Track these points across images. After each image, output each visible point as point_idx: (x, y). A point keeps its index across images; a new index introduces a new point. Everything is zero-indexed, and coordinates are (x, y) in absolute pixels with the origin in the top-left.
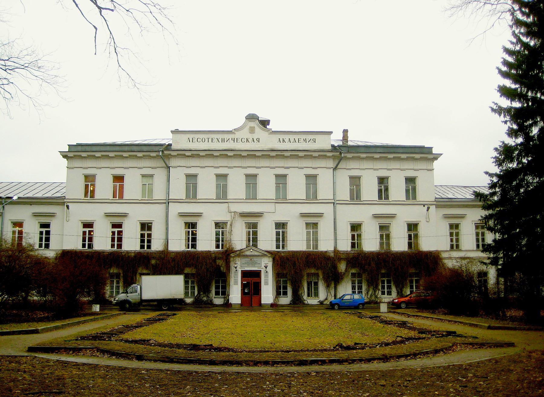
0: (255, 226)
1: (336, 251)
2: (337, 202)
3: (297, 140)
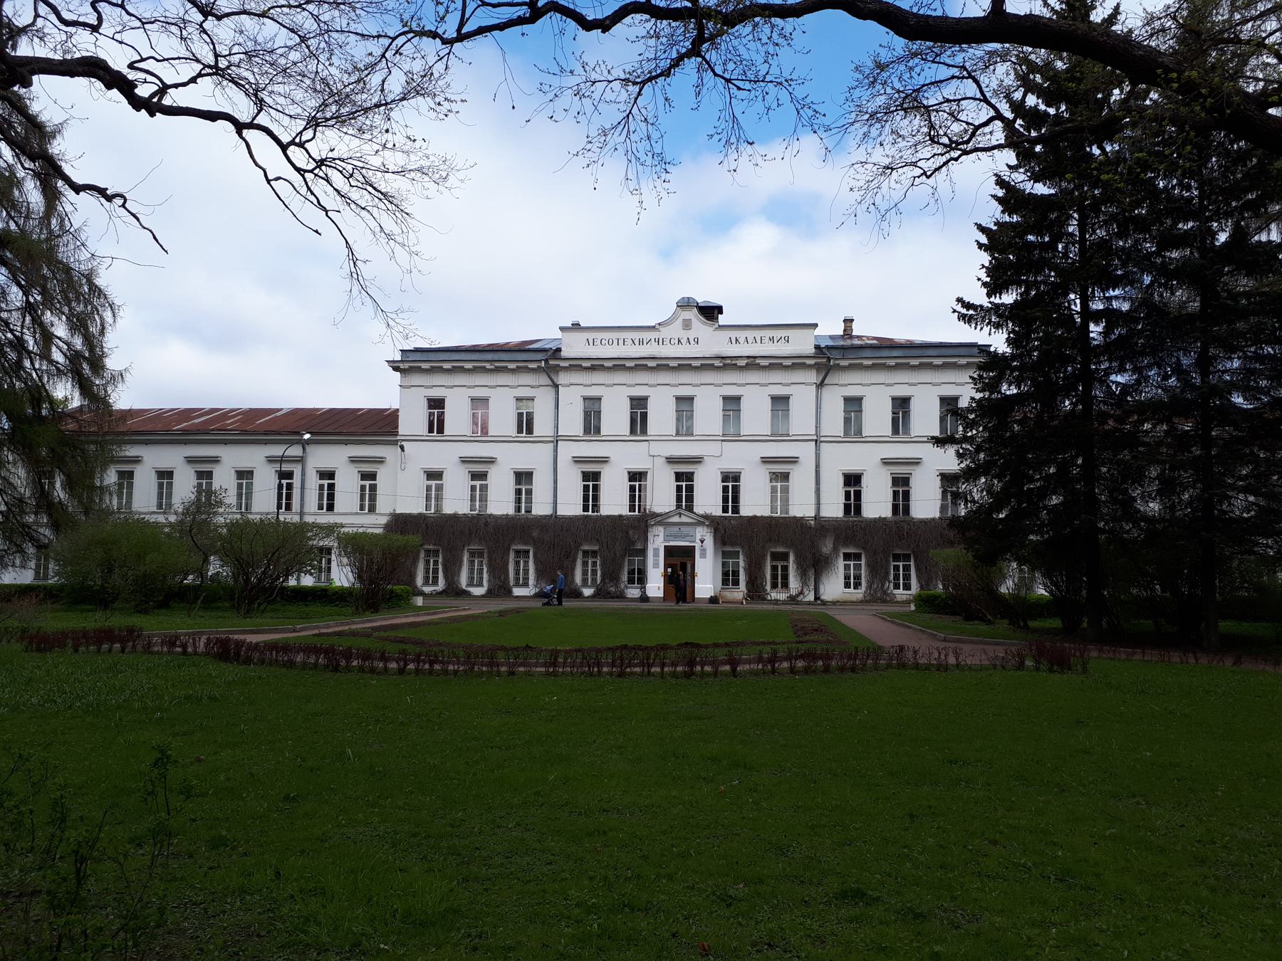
0: (689, 477)
1: (817, 517)
2: (822, 439)
3: (759, 341)
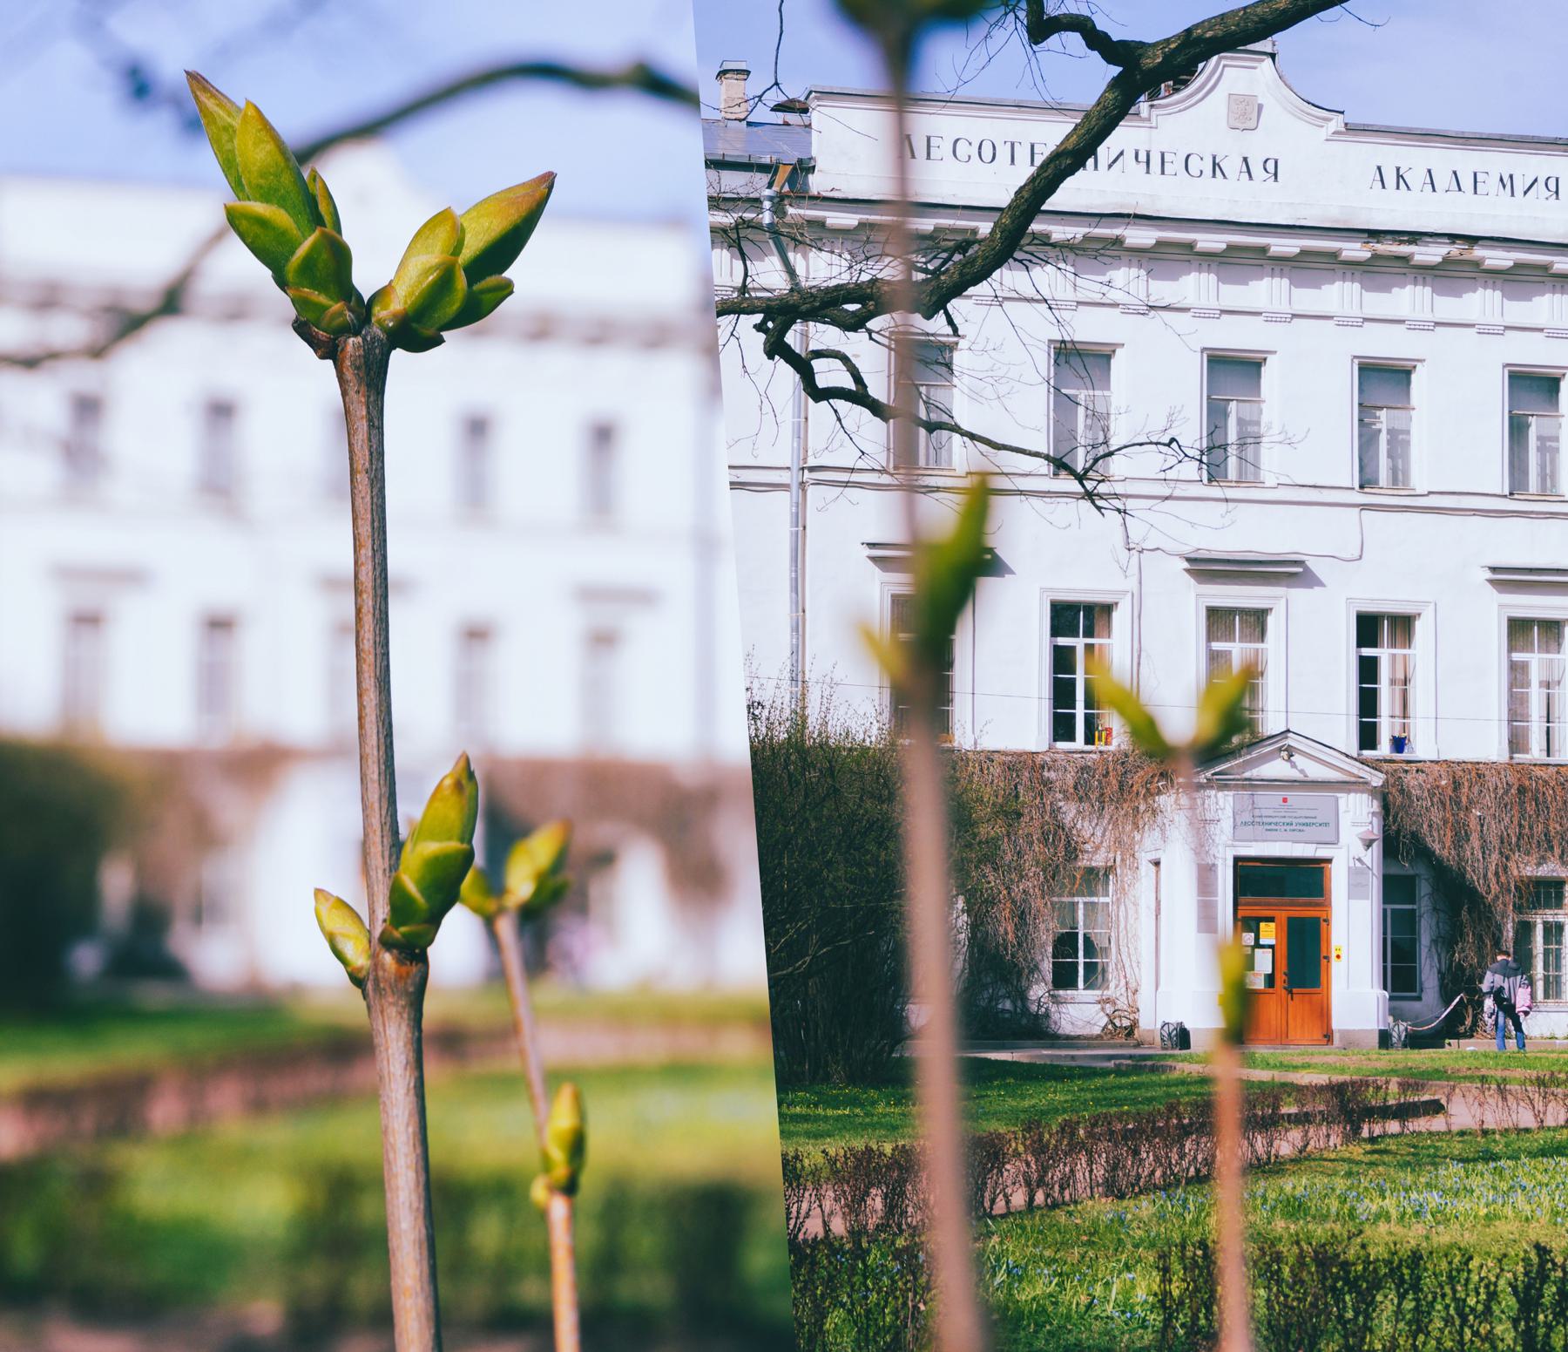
3: (1467, 183)
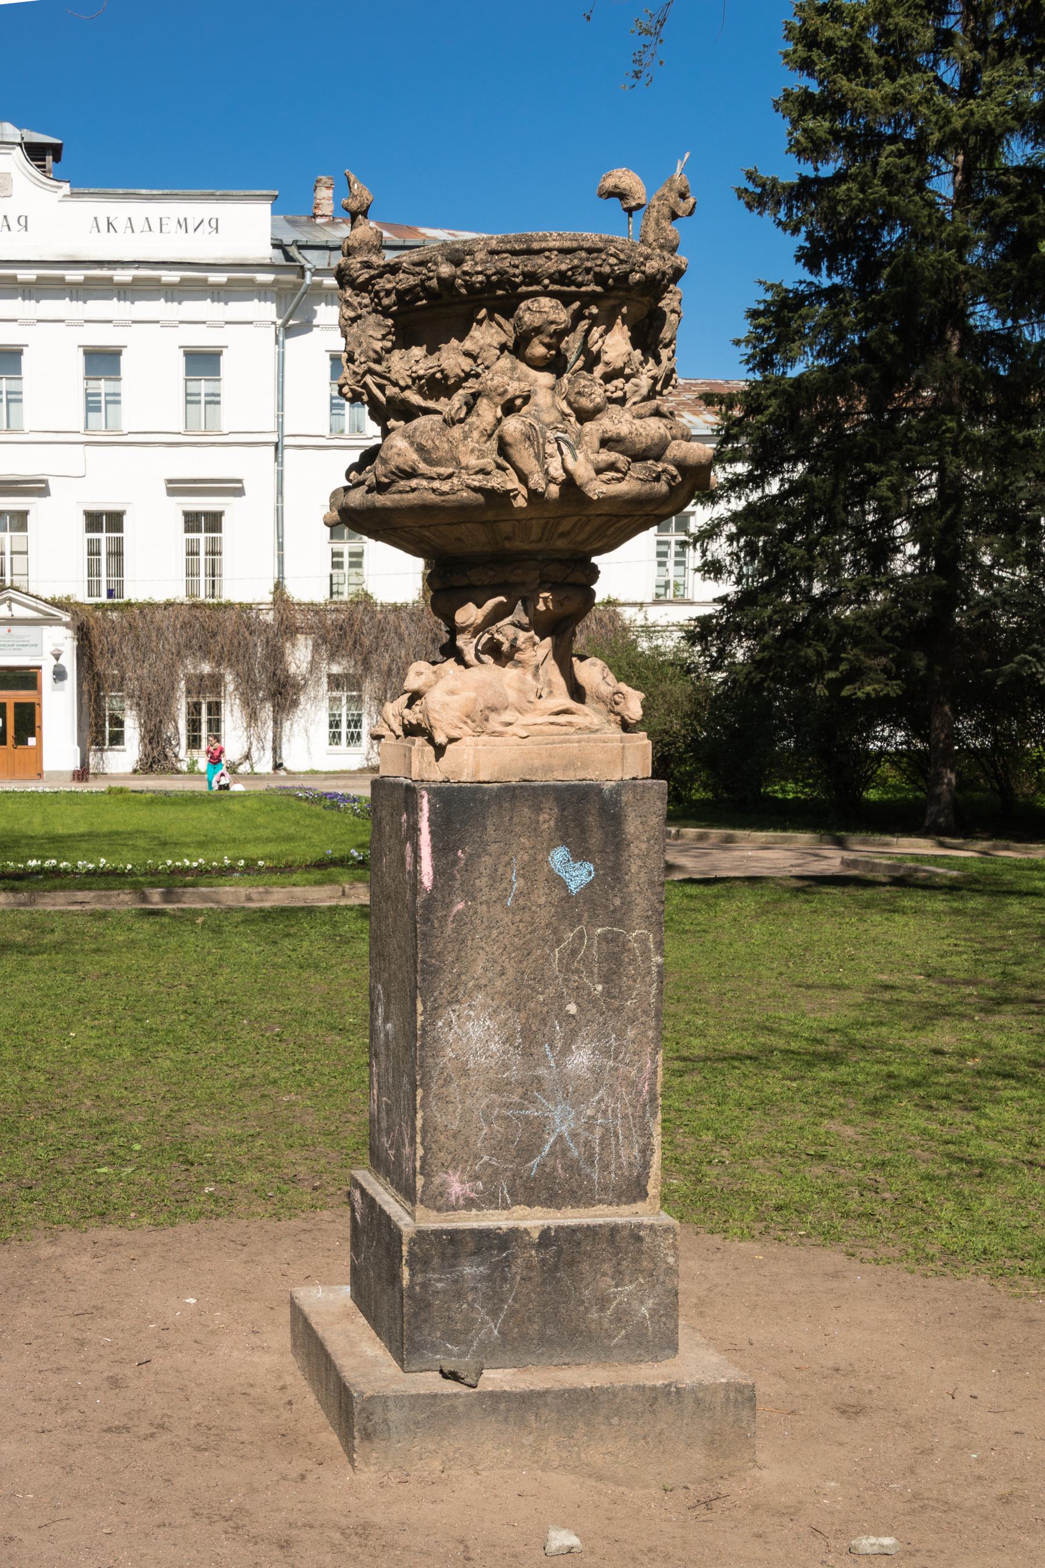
2: (287, 441)
3: (155, 226)
